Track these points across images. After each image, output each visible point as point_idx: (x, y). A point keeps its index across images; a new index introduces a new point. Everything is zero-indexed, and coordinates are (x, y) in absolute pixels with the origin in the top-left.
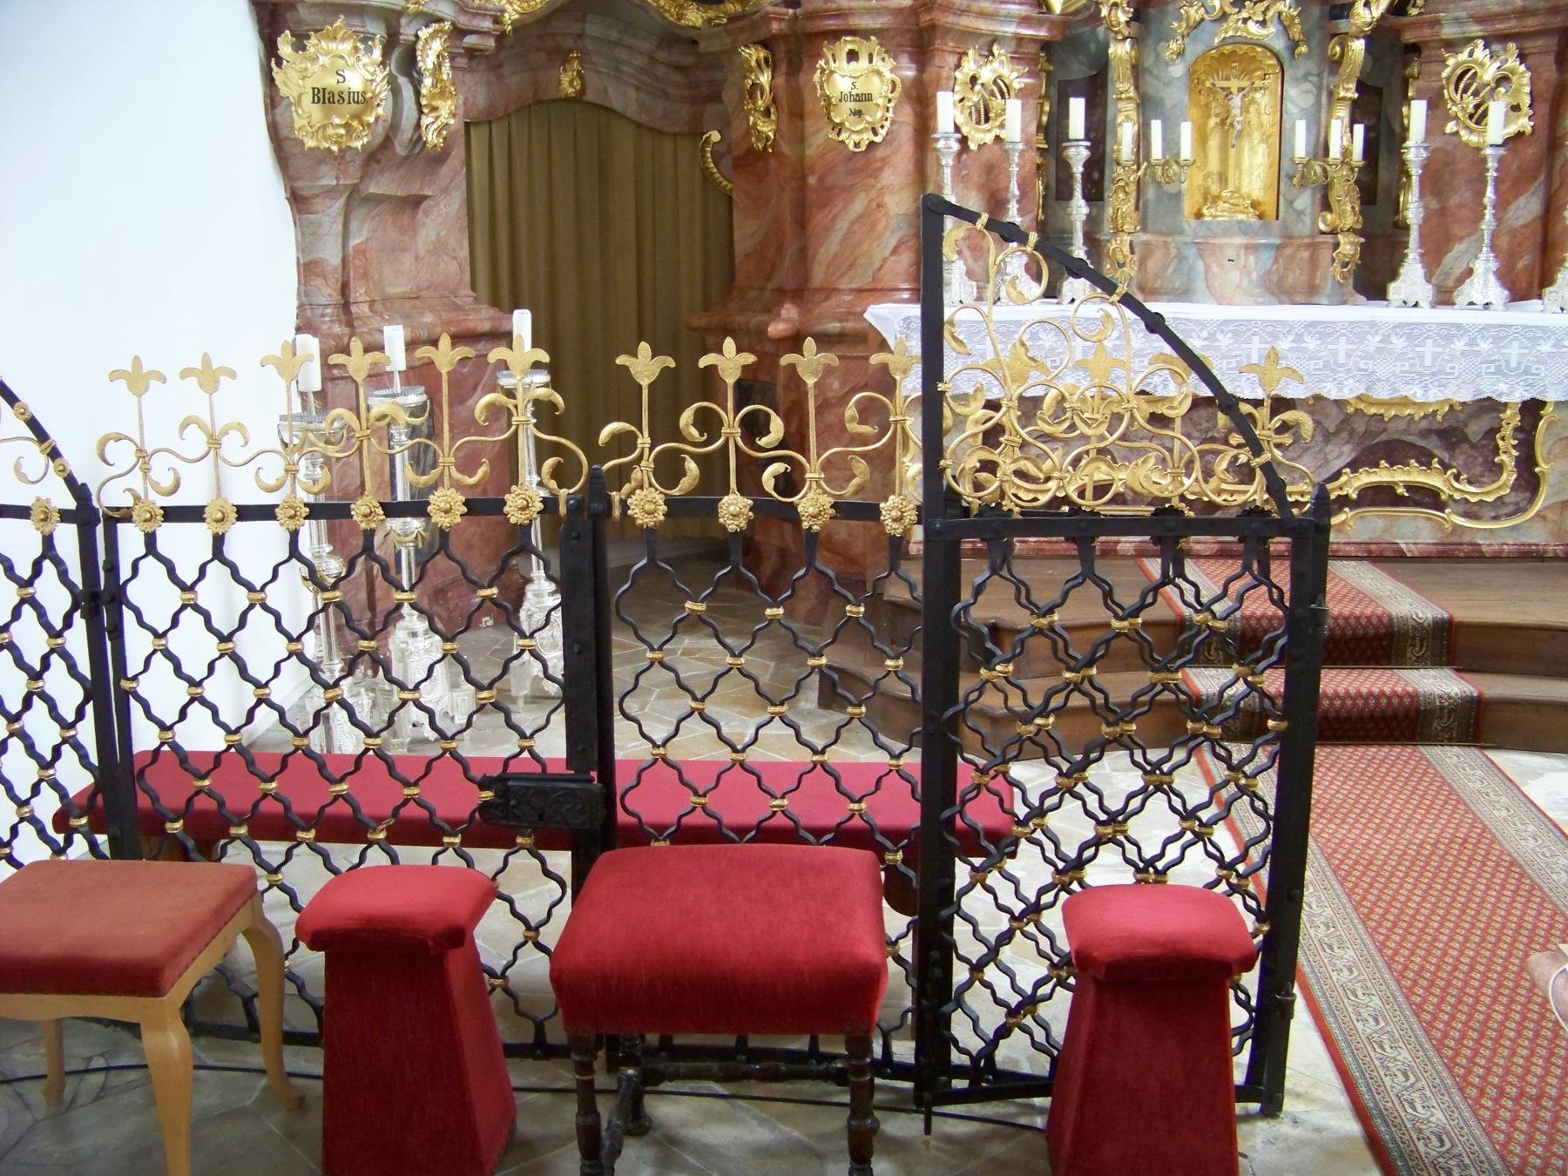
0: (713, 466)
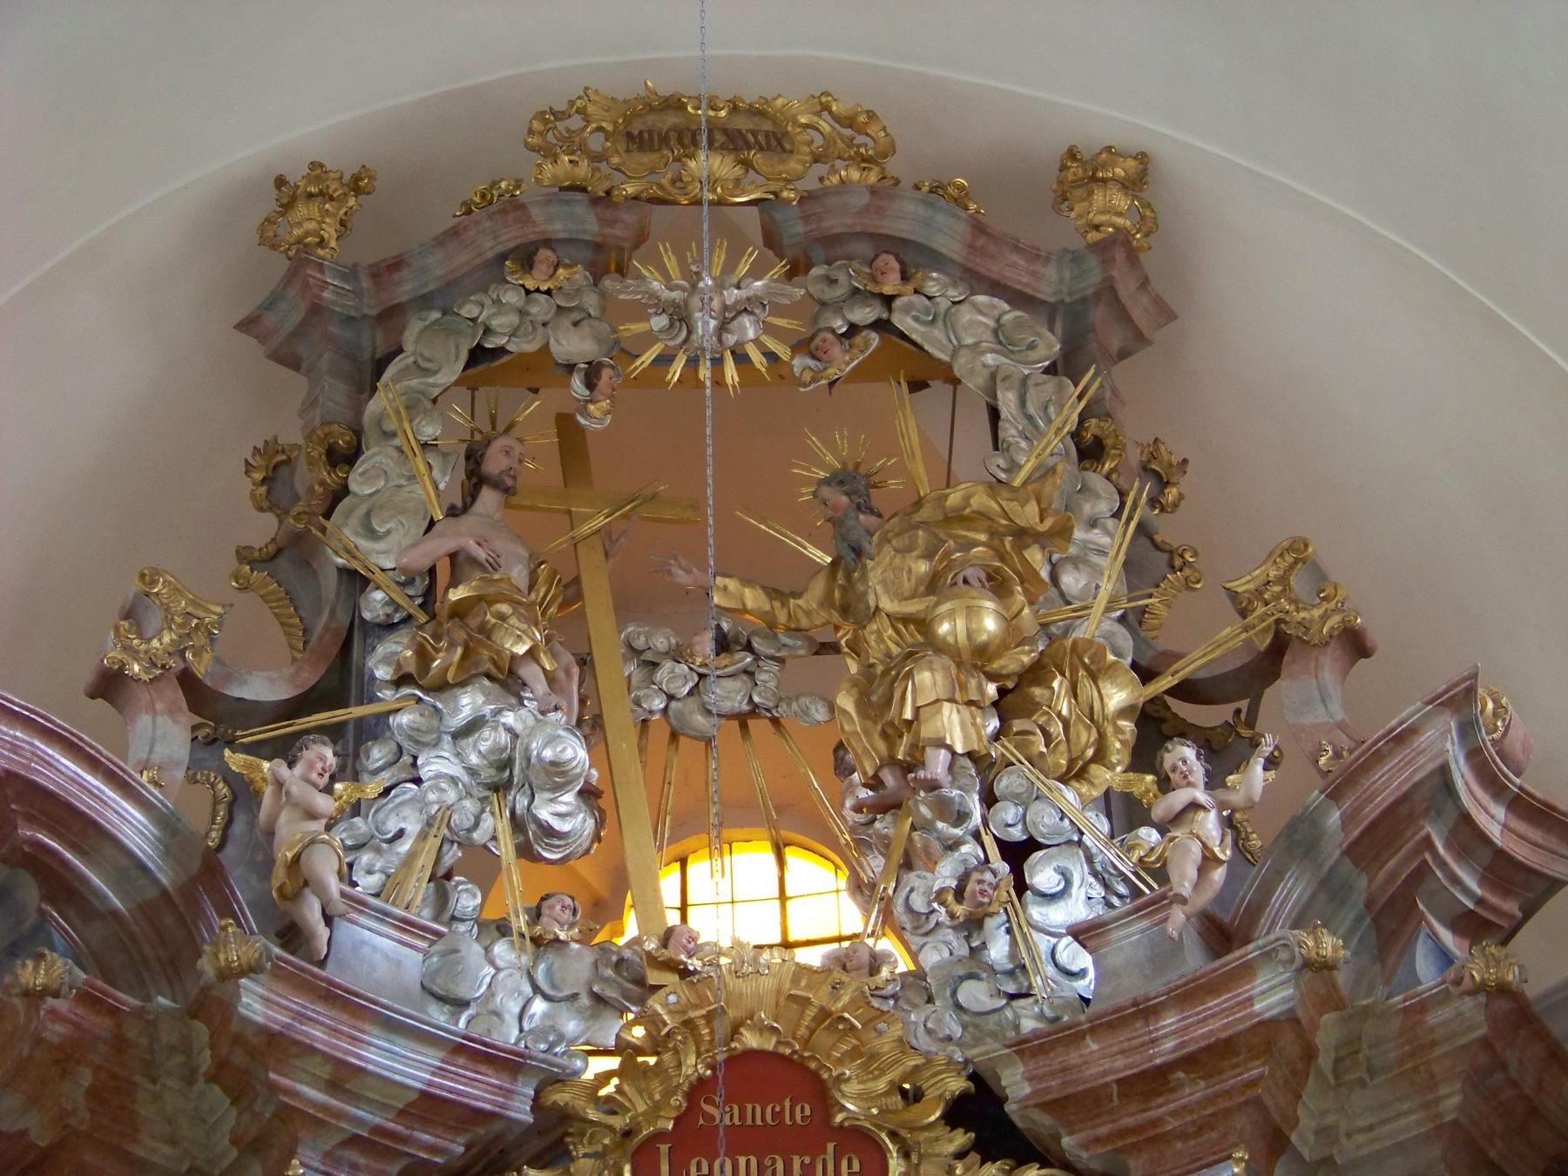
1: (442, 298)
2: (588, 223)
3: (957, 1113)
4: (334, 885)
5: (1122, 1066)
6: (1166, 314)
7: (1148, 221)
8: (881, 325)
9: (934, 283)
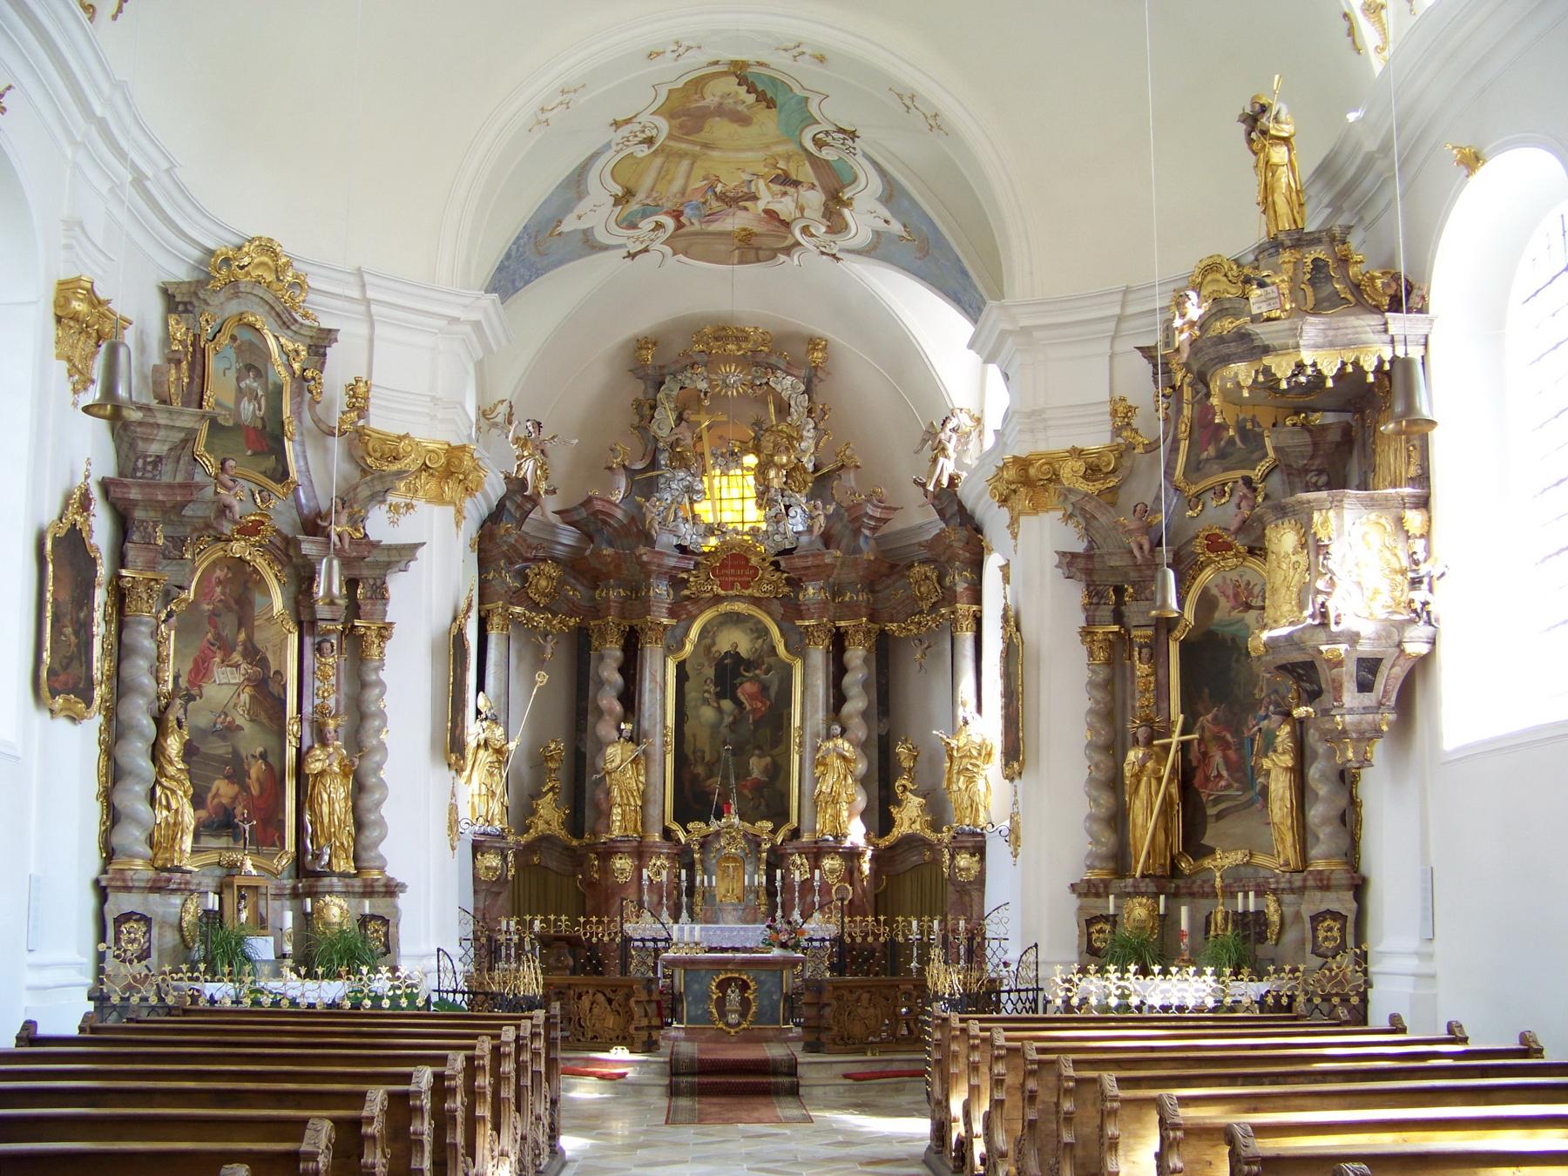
0: (592, 934)
1: (674, 374)
2: (706, 358)
3: (772, 563)
4: (657, 527)
5: (804, 565)
6: (829, 373)
7: (825, 360)
8: (767, 383)
9: (779, 373)
